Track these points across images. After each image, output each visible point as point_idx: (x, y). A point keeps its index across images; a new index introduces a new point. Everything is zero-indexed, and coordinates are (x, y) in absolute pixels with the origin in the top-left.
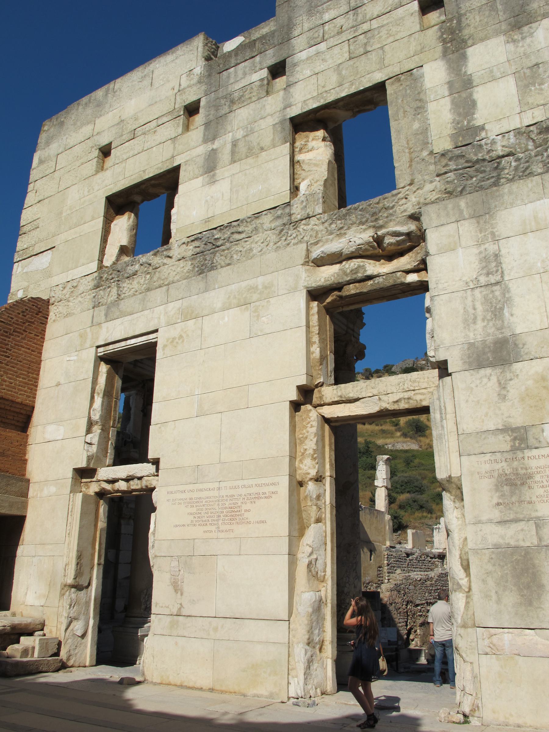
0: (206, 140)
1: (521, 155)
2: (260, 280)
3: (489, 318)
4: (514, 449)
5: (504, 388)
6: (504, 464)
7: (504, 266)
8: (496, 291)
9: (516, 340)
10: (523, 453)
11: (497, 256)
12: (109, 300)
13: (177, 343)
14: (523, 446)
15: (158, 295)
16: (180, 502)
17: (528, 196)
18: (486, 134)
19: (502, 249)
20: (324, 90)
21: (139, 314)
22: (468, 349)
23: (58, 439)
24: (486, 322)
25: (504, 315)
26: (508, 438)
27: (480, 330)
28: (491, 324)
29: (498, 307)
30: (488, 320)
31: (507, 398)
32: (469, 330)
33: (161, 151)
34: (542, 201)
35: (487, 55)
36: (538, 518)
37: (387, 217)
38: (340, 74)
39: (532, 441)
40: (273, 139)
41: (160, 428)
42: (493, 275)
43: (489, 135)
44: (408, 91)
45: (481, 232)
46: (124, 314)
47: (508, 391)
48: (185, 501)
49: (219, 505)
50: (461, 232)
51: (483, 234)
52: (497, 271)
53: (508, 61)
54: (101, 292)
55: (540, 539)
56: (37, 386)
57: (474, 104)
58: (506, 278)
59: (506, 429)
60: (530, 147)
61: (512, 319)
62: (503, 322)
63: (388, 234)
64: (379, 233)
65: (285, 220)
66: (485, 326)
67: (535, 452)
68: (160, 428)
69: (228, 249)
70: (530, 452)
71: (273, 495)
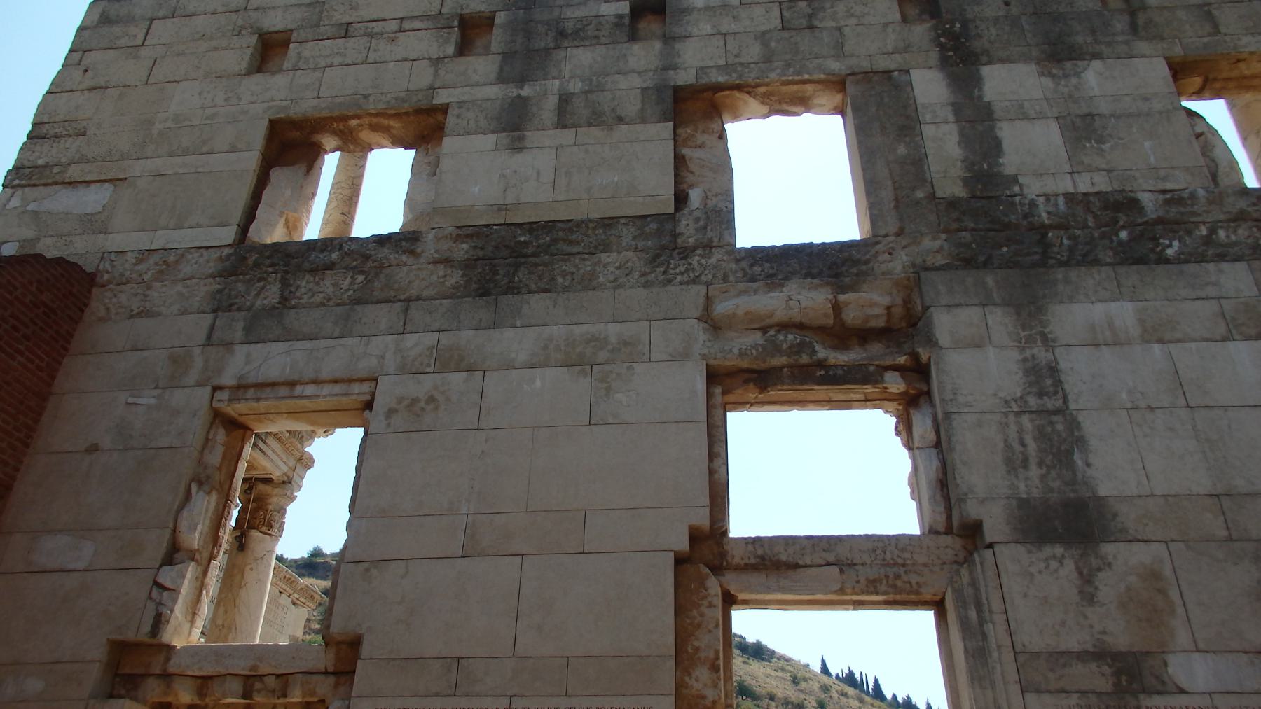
0: (502, 79)
1: (1078, 232)
2: (613, 330)
7: (1066, 386)
11: (1053, 370)
12: (259, 303)
13: (423, 409)
14: (1135, 686)
15: (382, 315)
17: (1096, 292)
18: (1021, 189)
20: (737, 60)
26: (1106, 669)
28: (1053, 473)
32: (1017, 476)
33: (407, 72)
35: (1007, 82)
37: (857, 275)
38: (765, 44)
40: (642, 110)
41: (367, 570)
43: (1026, 191)
44: (886, 100)
47: (1096, 588)
50: (990, 323)
52: (1056, 393)
53: (1047, 100)
54: (239, 284)
56: (27, 446)
57: (998, 144)
59: (1101, 654)
61: (1089, 472)
65: (666, 240)
68: (367, 570)
69: (545, 265)
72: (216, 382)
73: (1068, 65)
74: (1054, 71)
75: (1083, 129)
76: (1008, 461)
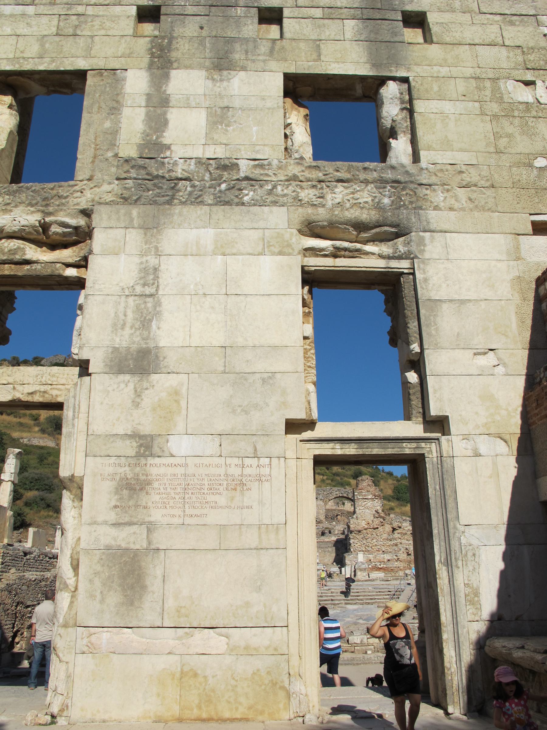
1: (197, 183)
3: (137, 327)
4: (139, 455)
5: (139, 396)
6: (127, 468)
7: (160, 281)
8: (148, 302)
9: (157, 353)
10: (146, 460)
11: (156, 270)
14: (147, 453)
17: (195, 222)
18: (171, 154)
19: (161, 264)
20: (21, 55)
22: (112, 352)
24: (134, 330)
25: (151, 326)
27: (127, 337)
28: (138, 333)
29: (147, 318)
30: (136, 328)
31: (140, 406)
32: (116, 334)
34: (206, 229)
35: (187, 82)
36: (150, 523)
37: (58, 206)
38: (42, 45)
39: (156, 450)
42: (149, 287)
43: (173, 155)
44: (108, 89)
45: (146, 243)
47: (142, 400)
50: (127, 239)
51: (147, 246)
52: (153, 284)
53: (205, 95)
55: (150, 543)
57: (166, 123)
58: (160, 292)
59: (135, 436)
60: (206, 178)
61: (158, 332)
62: (149, 333)
63: (56, 222)
64: (47, 220)
66: (132, 334)
67: (157, 460)
70: (152, 460)
74: (215, 77)
75: (220, 116)
76: (114, 325)
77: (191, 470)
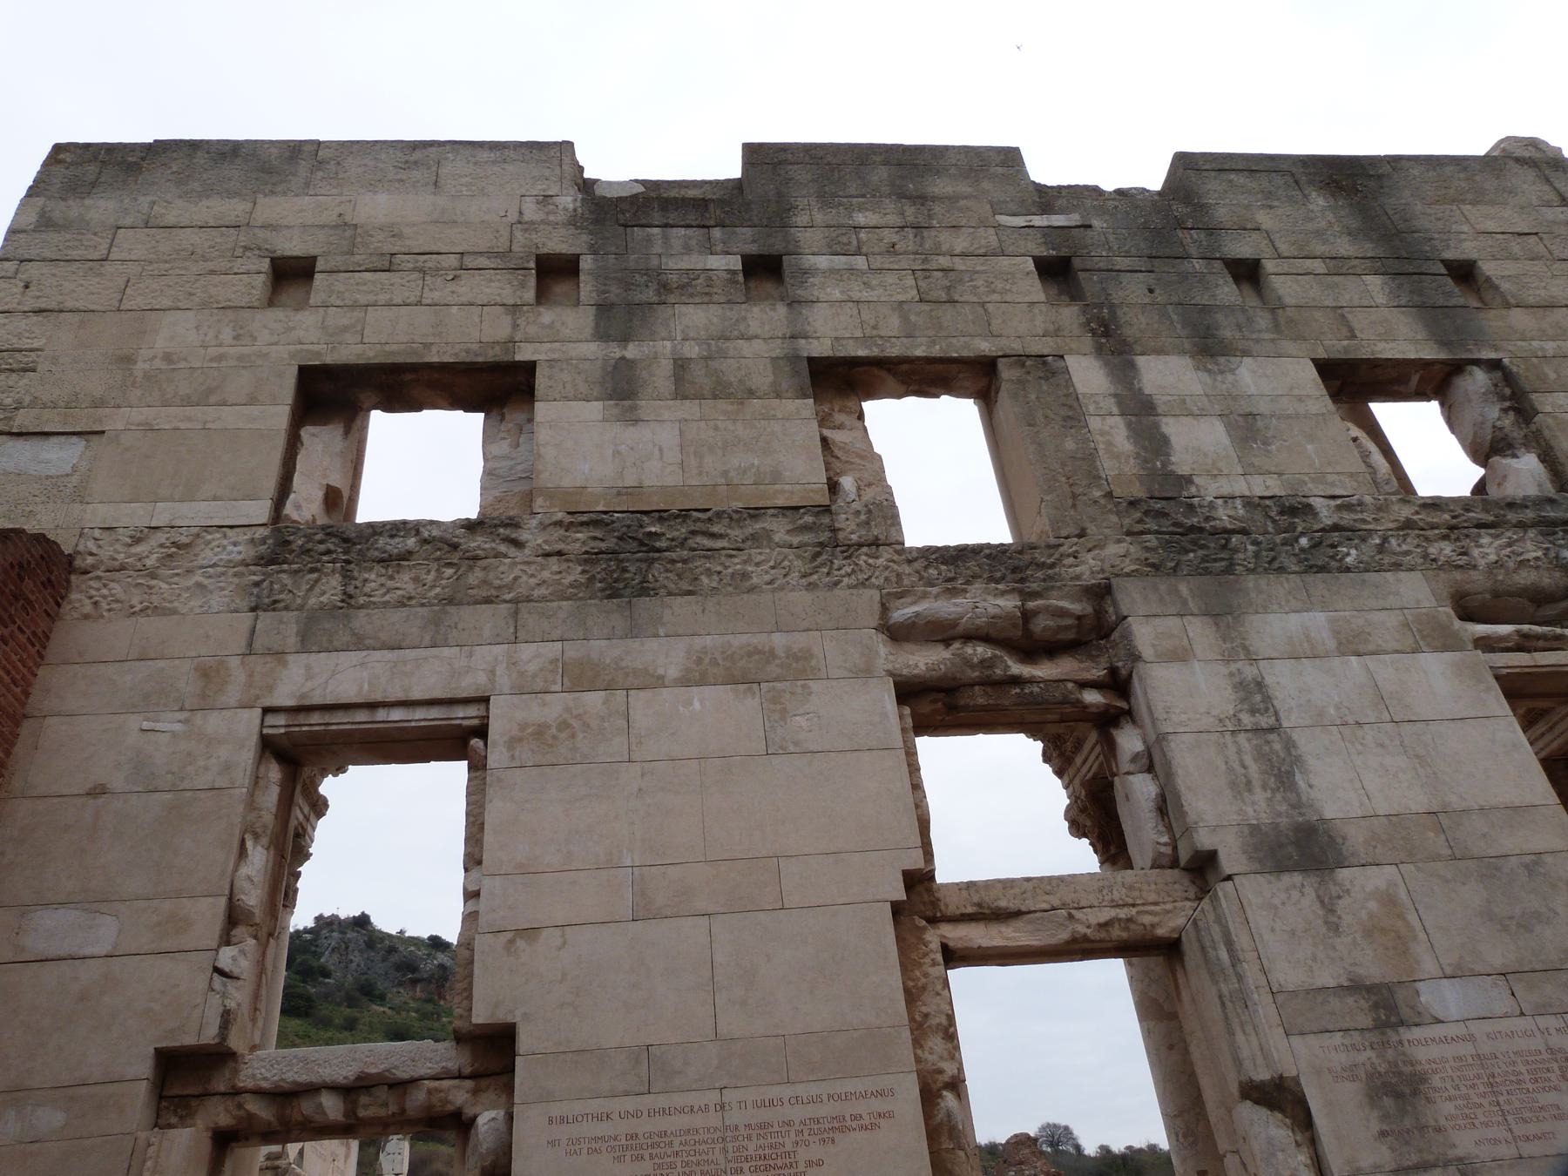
0: (601, 335)
1: (1261, 538)
2: (779, 640)
4: (1380, 1026)
6: (1369, 1053)
7: (1275, 703)
11: (1260, 685)
12: (312, 601)
13: (555, 737)
16: (594, 1145)
17: (1288, 601)
20: (875, 333)
21: (421, 652)
22: (1251, 834)
23: (88, 951)
27: (1264, 805)
28: (1279, 797)
33: (477, 320)
38: (905, 319)
40: (774, 384)
46: (359, 643)
48: (613, 1143)
49: (725, 1150)
52: (1267, 710)
54: (284, 576)
57: (1165, 441)
59: (1356, 987)
60: (1270, 529)
61: (1314, 794)
63: (1047, 608)
64: (1031, 604)
65: (824, 536)
67: (1417, 1033)
68: (511, 942)
69: (685, 561)
71: (882, 1121)
72: (268, 702)
73: (1222, 360)
75: (1247, 428)
76: (1233, 785)
77: (1486, 1048)
